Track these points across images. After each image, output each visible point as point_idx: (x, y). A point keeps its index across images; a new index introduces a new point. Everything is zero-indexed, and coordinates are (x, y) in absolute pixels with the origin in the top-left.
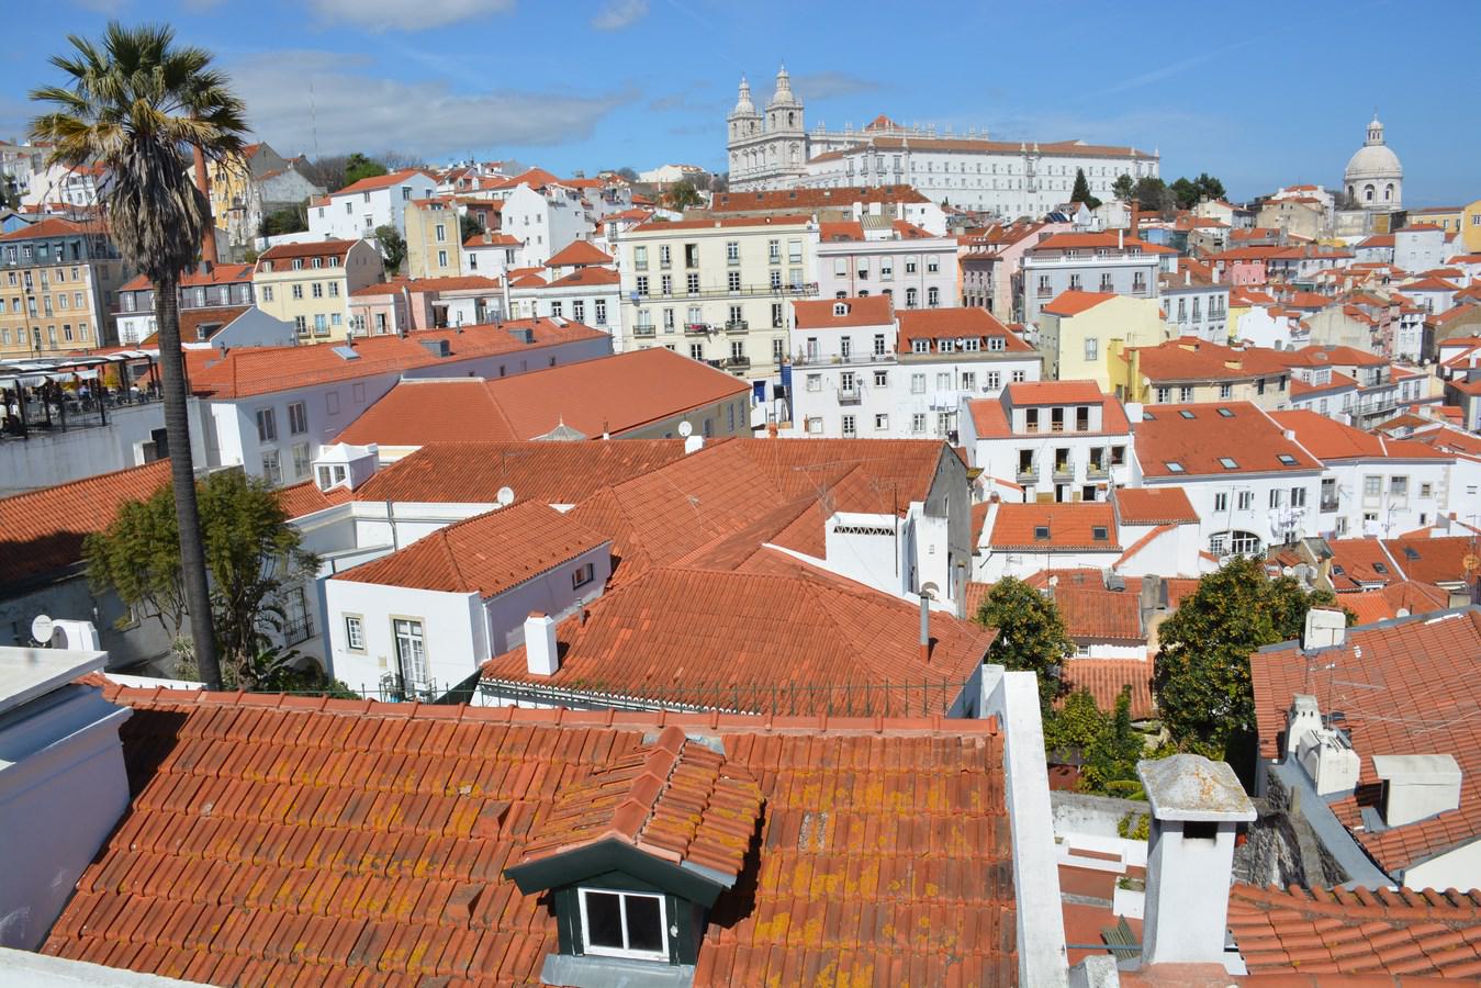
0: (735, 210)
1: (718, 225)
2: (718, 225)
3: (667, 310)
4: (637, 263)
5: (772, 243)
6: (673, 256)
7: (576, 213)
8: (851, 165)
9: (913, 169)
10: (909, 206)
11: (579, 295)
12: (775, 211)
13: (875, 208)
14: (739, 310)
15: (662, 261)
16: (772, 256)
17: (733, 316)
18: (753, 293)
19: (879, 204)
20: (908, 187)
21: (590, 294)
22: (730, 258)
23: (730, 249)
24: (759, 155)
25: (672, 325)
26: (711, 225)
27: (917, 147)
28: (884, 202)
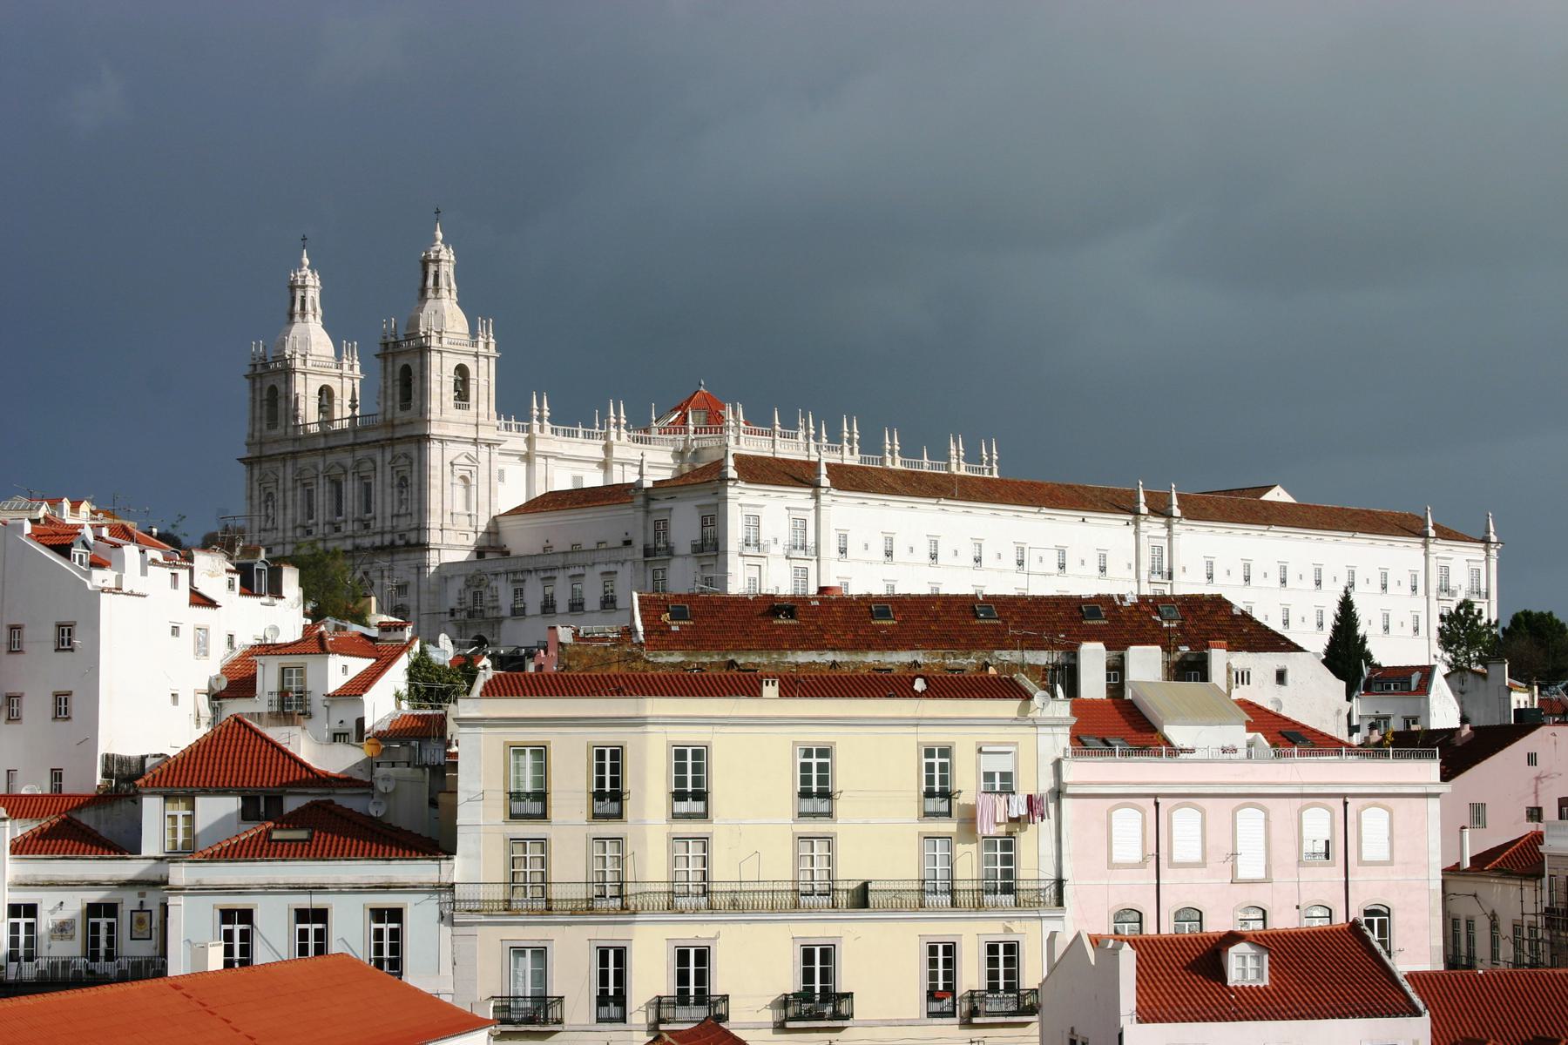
0: (717, 647)
1: (771, 690)
2: (771, 690)
3: (519, 952)
4: (515, 796)
5: (929, 753)
6: (629, 784)
7: (175, 631)
8: (661, 527)
9: (843, 551)
10: (1242, 660)
11: (320, 889)
12: (840, 657)
13: (1145, 664)
14: (827, 954)
15: (599, 796)
16: (930, 794)
17: (808, 976)
18: (738, 905)
19: (1158, 648)
20: (1219, 603)
21: (357, 889)
22: (805, 794)
23: (806, 768)
24: (351, 489)
25: (620, 999)
26: (748, 686)
27: (846, 479)
28: (1166, 649)
